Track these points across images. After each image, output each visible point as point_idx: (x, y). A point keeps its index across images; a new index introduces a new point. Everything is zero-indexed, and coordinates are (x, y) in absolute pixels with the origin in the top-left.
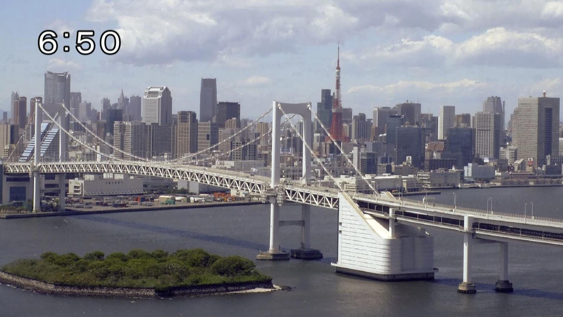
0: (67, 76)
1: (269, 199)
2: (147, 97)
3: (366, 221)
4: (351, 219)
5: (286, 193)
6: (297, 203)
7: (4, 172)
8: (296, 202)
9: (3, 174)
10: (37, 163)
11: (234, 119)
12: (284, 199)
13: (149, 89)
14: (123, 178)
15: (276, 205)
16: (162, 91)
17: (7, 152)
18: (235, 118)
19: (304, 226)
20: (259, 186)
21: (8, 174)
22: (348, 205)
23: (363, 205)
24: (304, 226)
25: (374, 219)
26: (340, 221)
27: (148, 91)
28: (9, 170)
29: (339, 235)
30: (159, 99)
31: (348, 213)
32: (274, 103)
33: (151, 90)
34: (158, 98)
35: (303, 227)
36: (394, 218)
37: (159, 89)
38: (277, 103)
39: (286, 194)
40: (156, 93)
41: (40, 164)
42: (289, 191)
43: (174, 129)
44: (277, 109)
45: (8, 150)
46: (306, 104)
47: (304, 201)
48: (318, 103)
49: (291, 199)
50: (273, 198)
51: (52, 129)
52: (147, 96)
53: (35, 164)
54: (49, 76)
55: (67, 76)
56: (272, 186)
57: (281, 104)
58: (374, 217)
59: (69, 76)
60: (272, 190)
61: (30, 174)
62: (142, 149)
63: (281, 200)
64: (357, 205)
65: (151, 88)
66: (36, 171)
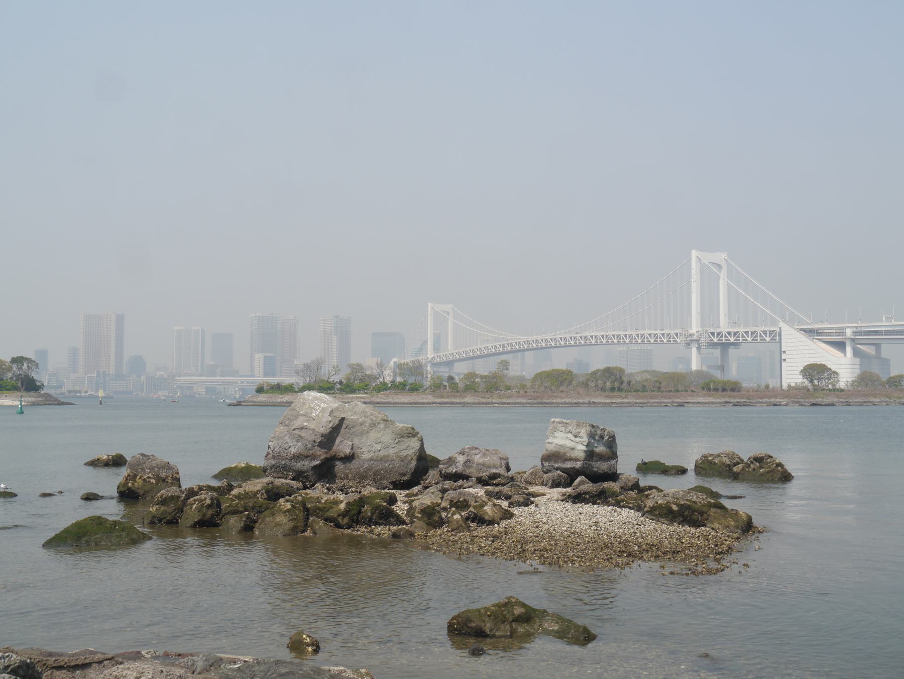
1: (689, 345)
3: (817, 345)
5: (709, 335)
8: (723, 343)
12: (709, 341)
15: (699, 348)
22: (793, 331)
29: (783, 363)
35: (722, 372)
36: (853, 337)
39: (710, 337)
42: (713, 334)
47: (732, 340)
49: (715, 340)
50: (694, 343)
53: (428, 356)
56: (693, 330)
60: (694, 334)
64: (802, 332)
66: (430, 362)
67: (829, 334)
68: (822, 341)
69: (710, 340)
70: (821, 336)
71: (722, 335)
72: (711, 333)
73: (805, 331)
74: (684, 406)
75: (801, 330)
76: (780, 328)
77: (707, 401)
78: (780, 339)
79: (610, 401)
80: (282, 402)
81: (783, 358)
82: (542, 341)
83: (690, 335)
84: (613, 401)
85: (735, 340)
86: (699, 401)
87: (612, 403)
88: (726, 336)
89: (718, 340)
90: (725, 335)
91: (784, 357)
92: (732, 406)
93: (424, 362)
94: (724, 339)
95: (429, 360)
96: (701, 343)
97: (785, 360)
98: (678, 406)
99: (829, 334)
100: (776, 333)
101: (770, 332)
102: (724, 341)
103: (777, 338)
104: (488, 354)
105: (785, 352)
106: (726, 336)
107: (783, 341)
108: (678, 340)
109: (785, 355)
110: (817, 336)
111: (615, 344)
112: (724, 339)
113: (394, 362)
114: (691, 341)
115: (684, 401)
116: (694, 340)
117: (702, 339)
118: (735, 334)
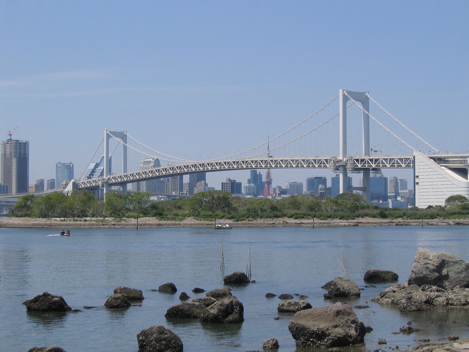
0: (72, 165)
2: (143, 165)
4: (429, 171)
5: (354, 161)
6: (367, 168)
7: (77, 188)
8: (365, 168)
9: (76, 188)
10: (107, 176)
11: (203, 181)
13: (144, 159)
14: (157, 200)
16: (154, 160)
17: (64, 186)
18: (204, 181)
19: (366, 191)
20: (327, 162)
21: (80, 189)
23: (439, 160)
24: (366, 191)
25: (449, 170)
26: (416, 175)
27: (143, 161)
28: (80, 186)
29: (416, 186)
30: (152, 166)
31: (426, 167)
32: (341, 91)
33: (146, 160)
34: (151, 165)
37: (152, 159)
38: (343, 90)
40: (149, 162)
41: (109, 177)
42: (357, 160)
43: (167, 184)
44: (344, 96)
45: (65, 184)
46: (366, 93)
47: (374, 166)
48: (248, 180)
49: (359, 166)
51: (99, 167)
52: (142, 165)
53: (105, 177)
54: (59, 165)
55: (72, 165)
57: (347, 91)
58: (449, 168)
59: (73, 165)
61: (100, 186)
62: (153, 191)
63: (351, 168)
65: (145, 159)
66: (106, 183)
67: (454, 162)
68: (449, 168)
69: (355, 166)
70: (447, 163)
71: (366, 160)
72: (355, 160)
73: (435, 159)
74: (358, 225)
75: (431, 158)
76: (414, 157)
77: (376, 221)
78: (414, 166)
79: (300, 222)
80: (33, 224)
81: (416, 181)
82: (208, 165)
83: (338, 161)
84: (303, 222)
85: (376, 166)
86: (369, 221)
87: (301, 223)
88: (368, 163)
89: (362, 166)
90: (368, 161)
91: (417, 180)
92: (395, 225)
93: (100, 183)
94: (366, 165)
95: (105, 181)
96: (348, 168)
97: (418, 183)
98: (354, 225)
99: (454, 162)
100: (410, 160)
101: (405, 159)
102: (366, 166)
103: (411, 165)
104: (158, 176)
105: (418, 176)
106: (368, 163)
107: (416, 167)
108: (328, 166)
109: (418, 179)
110: (444, 163)
111: (274, 168)
112: (366, 165)
113: (73, 182)
114: (339, 166)
115: (357, 221)
116: (342, 166)
117: (348, 165)
118: (376, 160)
